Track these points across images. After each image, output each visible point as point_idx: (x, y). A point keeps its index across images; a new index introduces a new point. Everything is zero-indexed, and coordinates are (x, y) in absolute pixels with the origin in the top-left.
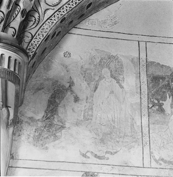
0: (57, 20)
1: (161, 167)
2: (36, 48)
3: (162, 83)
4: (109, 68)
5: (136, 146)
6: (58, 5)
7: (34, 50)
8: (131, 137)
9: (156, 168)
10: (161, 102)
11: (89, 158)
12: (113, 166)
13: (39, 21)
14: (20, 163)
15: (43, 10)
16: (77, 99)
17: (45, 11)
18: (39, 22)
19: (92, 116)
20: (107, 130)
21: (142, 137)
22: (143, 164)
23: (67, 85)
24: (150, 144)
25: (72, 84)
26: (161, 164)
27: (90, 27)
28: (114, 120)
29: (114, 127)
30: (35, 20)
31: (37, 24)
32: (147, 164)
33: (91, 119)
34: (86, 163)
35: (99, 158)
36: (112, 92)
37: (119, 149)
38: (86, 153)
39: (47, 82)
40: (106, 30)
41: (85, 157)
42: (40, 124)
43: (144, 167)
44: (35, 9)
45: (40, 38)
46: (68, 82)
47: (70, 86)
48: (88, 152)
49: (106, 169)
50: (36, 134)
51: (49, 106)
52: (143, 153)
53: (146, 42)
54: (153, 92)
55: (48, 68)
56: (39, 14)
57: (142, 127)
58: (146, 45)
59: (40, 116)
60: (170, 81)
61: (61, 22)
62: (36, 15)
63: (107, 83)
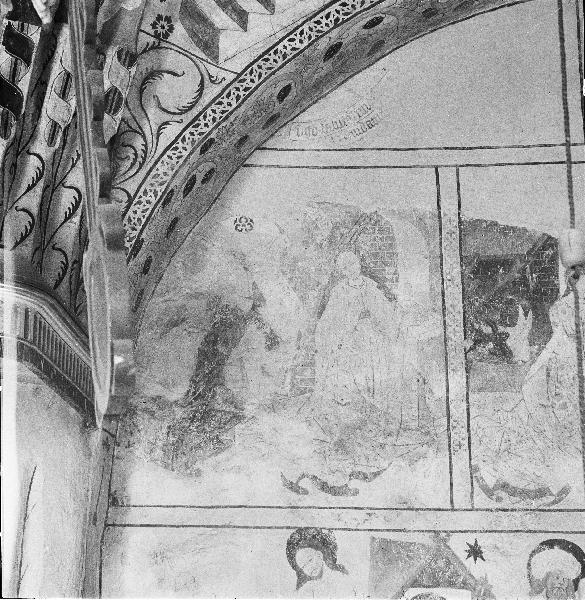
0: (189, 148)
1: (499, 505)
2: (139, 228)
3: (502, 278)
4: (357, 251)
5: (431, 452)
6: (190, 108)
7: (136, 233)
8: (419, 433)
9: (487, 510)
10: (501, 329)
11: (306, 492)
12: (370, 511)
13: (146, 156)
14: (134, 515)
15: (155, 128)
17: (160, 129)
18: (144, 159)
19: (313, 380)
20: (351, 416)
21: (448, 429)
22: (452, 502)
23: (246, 306)
24: (469, 447)
25: (258, 301)
26: (499, 499)
27: (302, 141)
28: (371, 387)
29: (372, 406)
30: (136, 154)
31: (140, 168)
33: (311, 391)
34: (298, 508)
36: (366, 314)
37: (385, 464)
38: (300, 479)
39: (194, 303)
40: (346, 145)
41: (297, 492)
42: (179, 413)
43: (453, 510)
44: (134, 126)
45: (148, 202)
46: (250, 298)
47: (254, 307)
48: (303, 476)
49: (351, 518)
50: (172, 439)
51: (200, 365)
52: (451, 473)
53: (458, 167)
54: (477, 304)
55: (195, 265)
56: (145, 141)
57: (448, 403)
58: (458, 175)
59: (177, 393)
60: (528, 270)
61: (203, 151)
62: (139, 143)
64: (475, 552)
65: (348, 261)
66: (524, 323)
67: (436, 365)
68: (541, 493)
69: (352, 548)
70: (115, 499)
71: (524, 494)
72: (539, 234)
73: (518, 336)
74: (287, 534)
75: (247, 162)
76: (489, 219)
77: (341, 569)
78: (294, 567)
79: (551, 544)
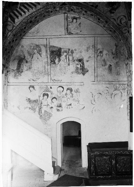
16: (27, 62)
19: (31, 67)
23: (23, 57)
25: (25, 57)
32: (49, 81)
36: (38, 58)
39: (17, 57)
47: (24, 58)
55: (17, 52)
59: (15, 69)
63: (36, 56)
64: (51, 88)
67: (47, 65)
68: (59, 80)
71: (57, 80)
73: (57, 61)
74: (29, 86)
79: (60, 87)
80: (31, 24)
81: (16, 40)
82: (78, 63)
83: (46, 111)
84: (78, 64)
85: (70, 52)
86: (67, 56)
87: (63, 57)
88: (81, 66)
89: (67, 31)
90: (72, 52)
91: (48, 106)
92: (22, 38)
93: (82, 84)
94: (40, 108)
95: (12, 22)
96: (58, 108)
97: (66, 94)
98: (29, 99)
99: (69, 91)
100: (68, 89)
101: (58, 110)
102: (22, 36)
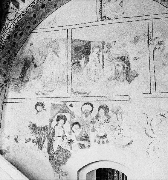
3: (80, 50)
10: (79, 61)
11: (39, 95)
14: (8, 101)
16: (36, 66)
23: (31, 60)
25: (33, 59)
26: (76, 95)
27: (42, 27)
35: (44, 94)
42: (18, 81)
49: (48, 100)
63: (51, 55)
64: (71, 106)
65: (50, 50)
66: (84, 59)
67: (66, 69)
68: (85, 93)
69: (47, 106)
70: (6, 98)
71: (81, 93)
72: (87, 41)
73: (82, 62)
75: (32, 32)
76: (77, 39)
77: (45, 110)
78: (36, 109)
79: (86, 103)
80: (44, 10)
81: (21, 34)
82: (118, 63)
83: (60, 147)
84: (118, 65)
85: (105, 46)
86: (101, 53)
87: (93, 56)
88: (124, 68)
89: (101, 15)
90: (109, 47)
91: (65, 138)
92: (31, 32)
93: (127, 98)
94: (51, 142)
95: (16, 8)
96: (82, 142)
97: (97, 116)
98: (34, 125)
99: (102, 111)
100: (101, 108)
101: (82, 146)
102: (31, 29)
